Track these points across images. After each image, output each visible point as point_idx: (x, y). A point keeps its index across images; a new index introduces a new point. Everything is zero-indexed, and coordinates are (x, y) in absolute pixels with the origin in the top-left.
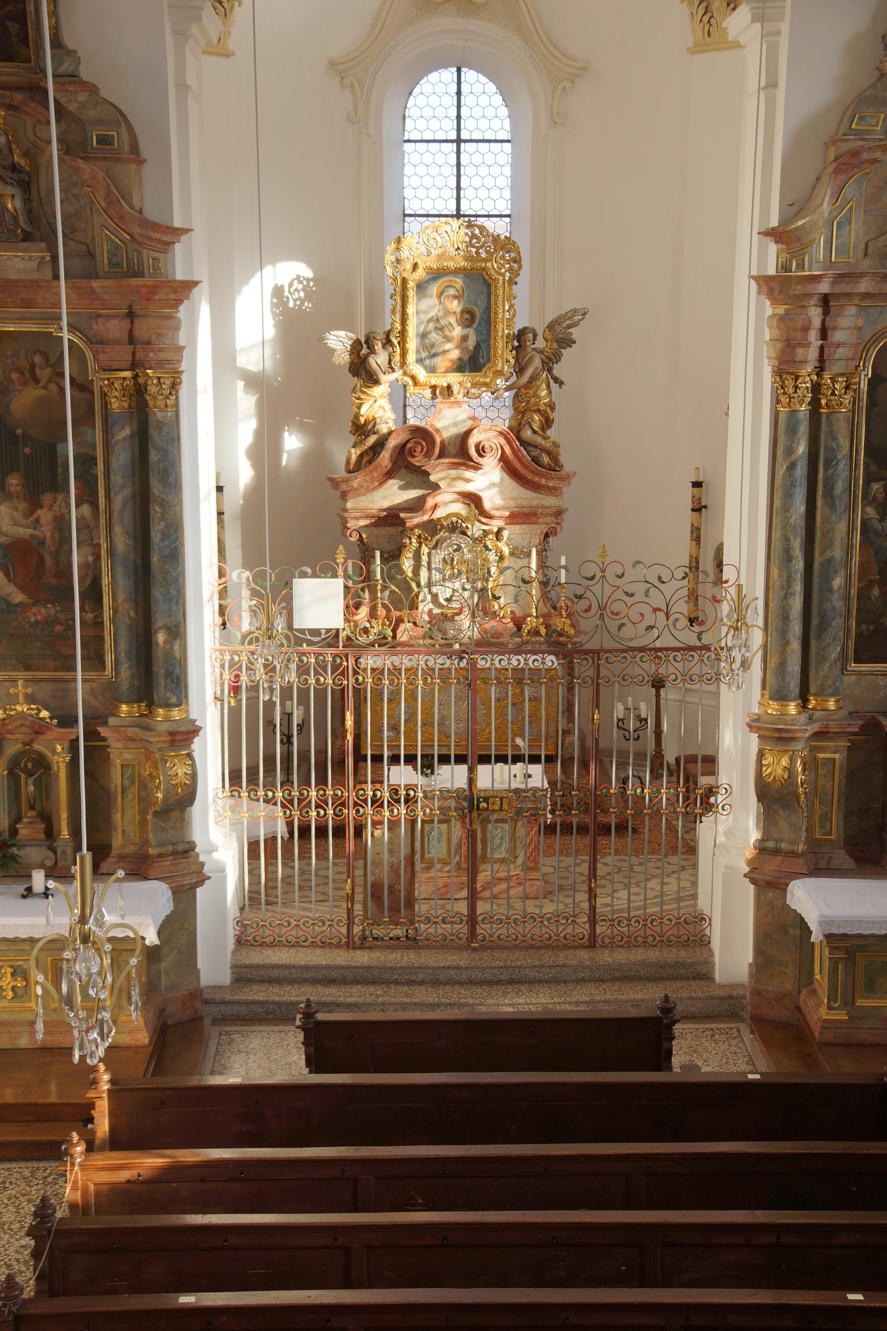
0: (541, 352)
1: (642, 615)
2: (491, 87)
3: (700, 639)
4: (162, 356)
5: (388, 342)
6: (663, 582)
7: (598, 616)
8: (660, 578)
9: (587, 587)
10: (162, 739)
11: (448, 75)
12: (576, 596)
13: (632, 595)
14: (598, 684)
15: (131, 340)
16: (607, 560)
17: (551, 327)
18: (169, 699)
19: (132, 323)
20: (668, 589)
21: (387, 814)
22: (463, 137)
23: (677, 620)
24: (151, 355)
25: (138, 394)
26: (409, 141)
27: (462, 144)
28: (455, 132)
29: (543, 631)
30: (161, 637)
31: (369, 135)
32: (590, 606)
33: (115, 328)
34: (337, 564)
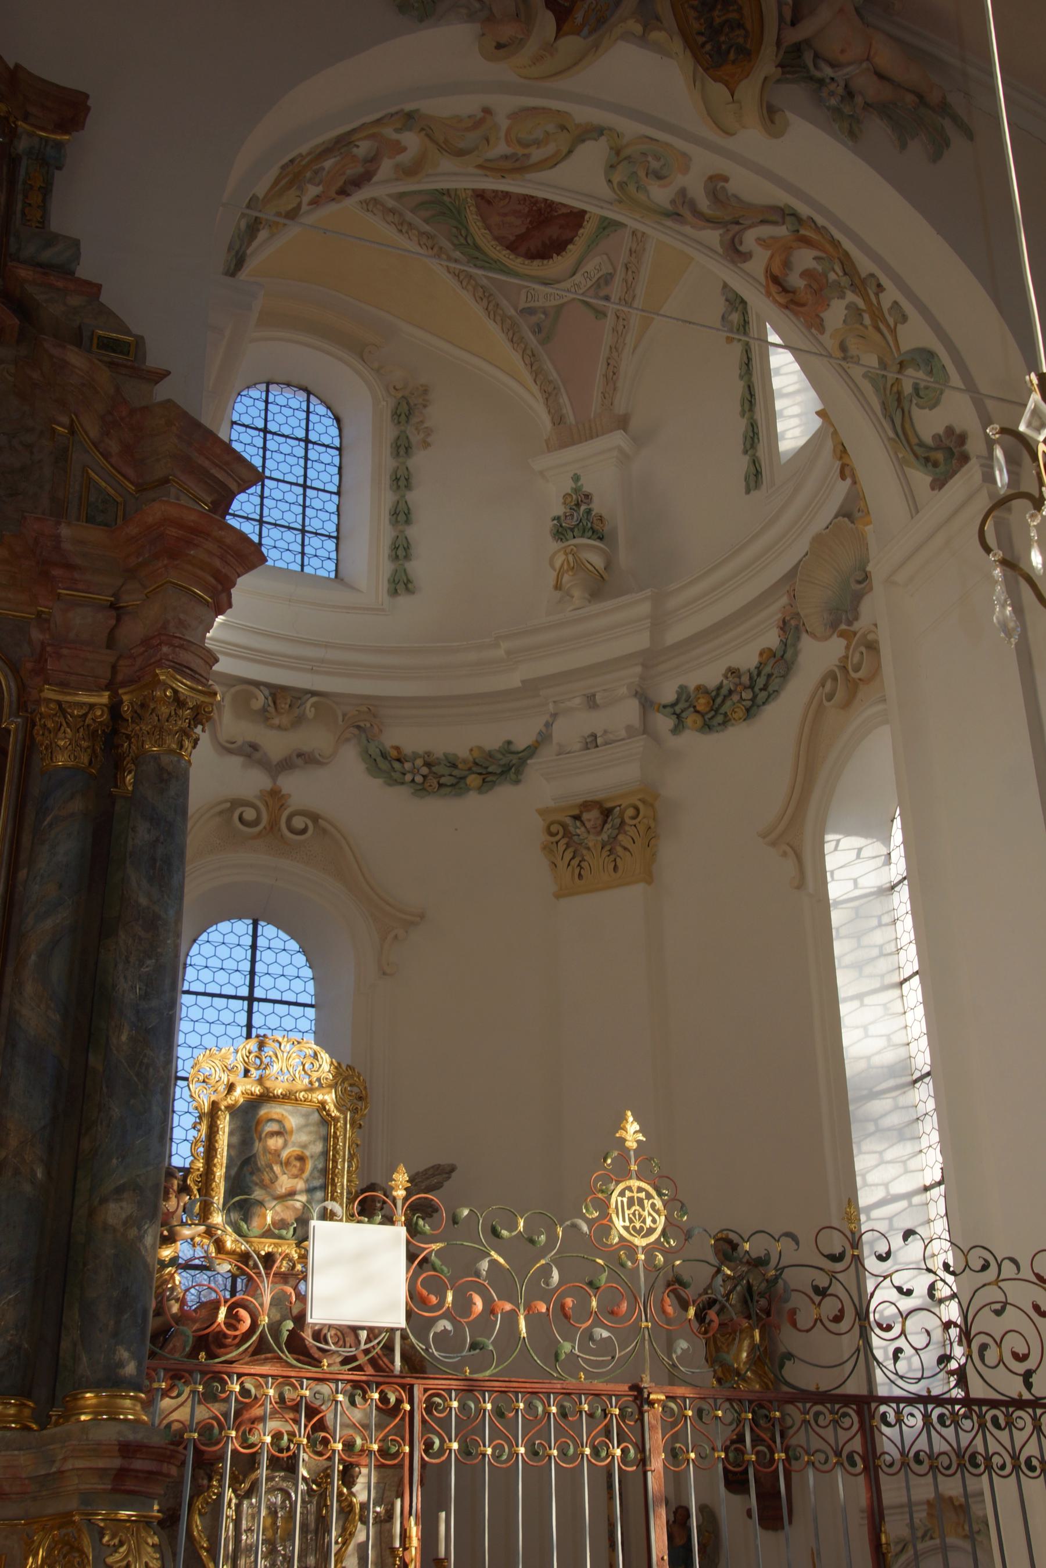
1: (928, 1333)
3: (1029, 1386)
4: (185, 657)
5: (184, 1189)
9: (832, 1276)
10: (101, 1464)
11: (242, 927)
12: (817, 1290)
13: (909, 1293)
15: (111, 642)
18: (121, 1364)
19: (118, 619)
22: (258, 993)
23: (983, 1347)
24: (165, 649)
25: (111, 738)
26: (188, 992)
27: (255, 1004)
28: (247, 989)
30: (116, 1212)
32: (842, 1311)
33: (84, 621)
34: (394, 1200)
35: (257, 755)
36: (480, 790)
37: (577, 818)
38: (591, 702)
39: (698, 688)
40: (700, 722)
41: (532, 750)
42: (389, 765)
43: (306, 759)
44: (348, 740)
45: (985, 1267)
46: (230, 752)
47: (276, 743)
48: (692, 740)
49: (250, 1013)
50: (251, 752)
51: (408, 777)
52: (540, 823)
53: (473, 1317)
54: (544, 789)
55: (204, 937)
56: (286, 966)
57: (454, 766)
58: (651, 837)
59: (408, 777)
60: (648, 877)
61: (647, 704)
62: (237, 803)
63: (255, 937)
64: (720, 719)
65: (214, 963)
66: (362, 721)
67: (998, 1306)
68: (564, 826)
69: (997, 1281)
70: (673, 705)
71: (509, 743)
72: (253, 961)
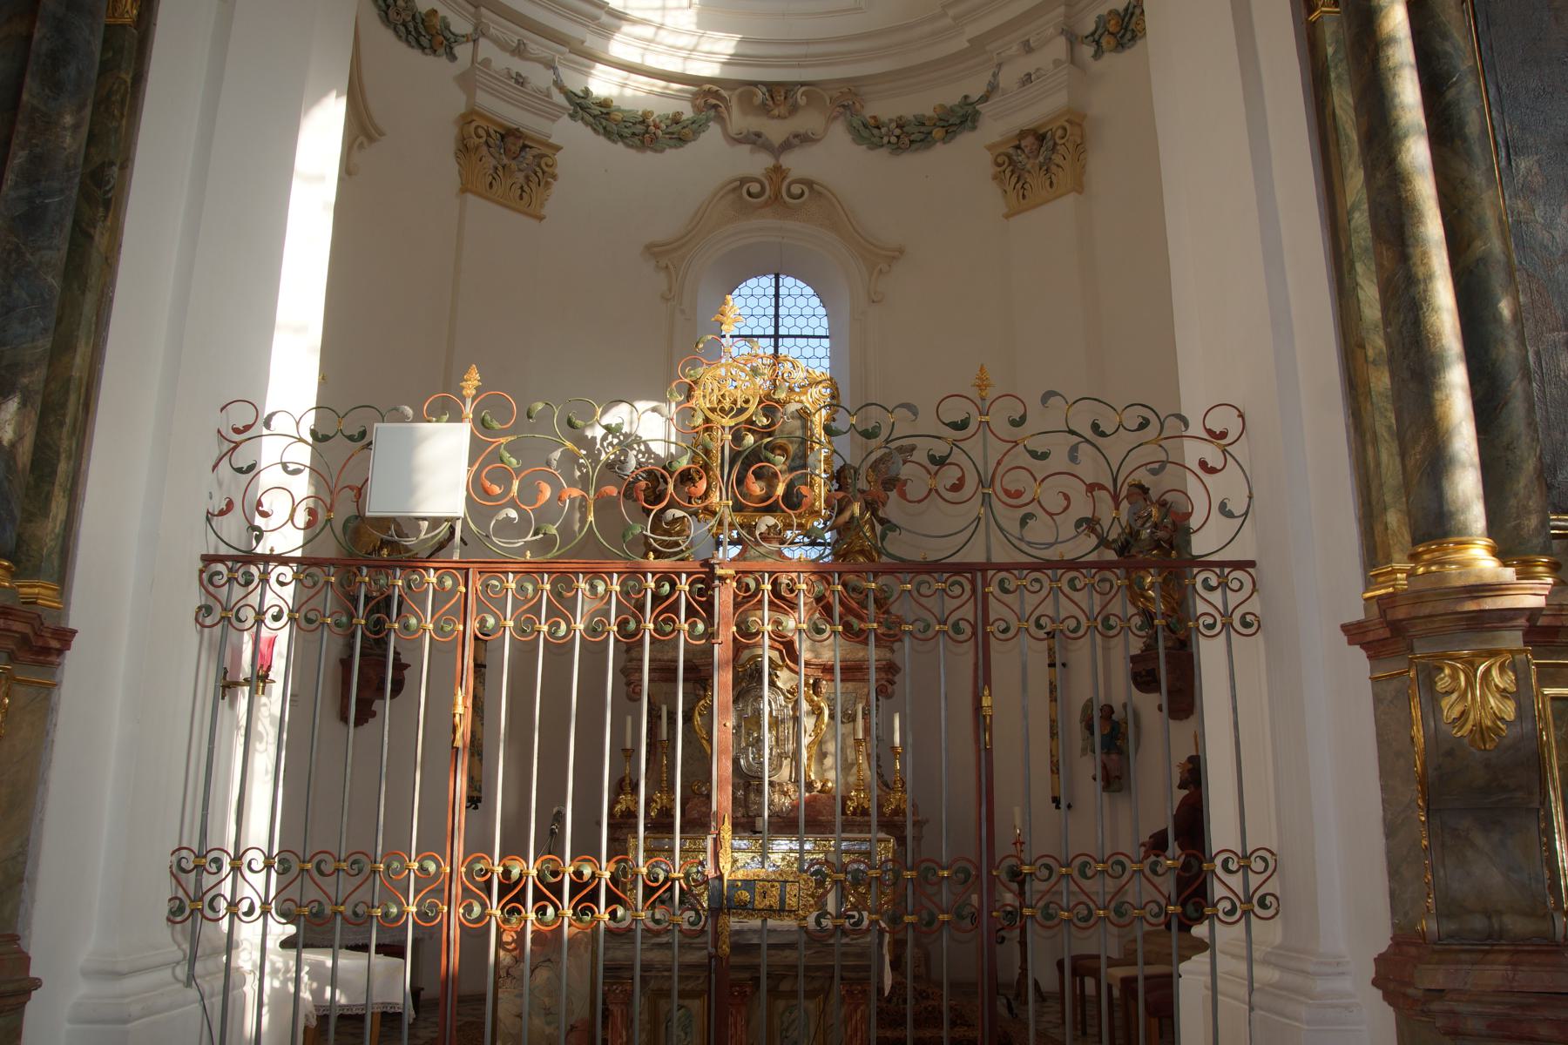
0: (862, 492)
1: (1067, 497)
2: (809, 291)
6: (1103, 435)
7: (979, 497)
8: (1095, 427)
9: (955, 443)
11: (767, 282)
12: (932, 459)
13: (1044, 456)
14: (986, 635)
16: (991, 394)
17: (874, 466)
20: (1115, 447)
21: (532, 916)
22: (782, 331)
29: (874, 811)
31: (683, 311)
32: (962, 480)
35: (760, 141)
36: (944, 141)
37: (1018, 147)
38: (1028, 48)
39: (1110, 12)
40: (1113, 42)
41: (985, 98)
42: (869, 133)
43: (804, 139)
44: (835, 118)
45: (1144, 424)
46: (739, 141)
47: (776, 131)
48: (1111, 60)
49: (776, 347)
50: (755, 140)
51: (885, 140)
52: (988, 158)
53: (539, 504)
54: (996, 127)
55: (736, 292)
56: (803, 307)
57: (923, 124)
58: (1080, 149)
59: (885, 140)
60: (1079, 187)
61: (1073, 39)
62: (743, 181)
63: (777, 287)
64: (1129, 35)
65: (747, 311)
66: (845, 101)
67: (1156, 466)
68: (1009, 157)
69: (1157, 441)
70: (1093, 34)
71: (966, 97)
72: (777, 307)
